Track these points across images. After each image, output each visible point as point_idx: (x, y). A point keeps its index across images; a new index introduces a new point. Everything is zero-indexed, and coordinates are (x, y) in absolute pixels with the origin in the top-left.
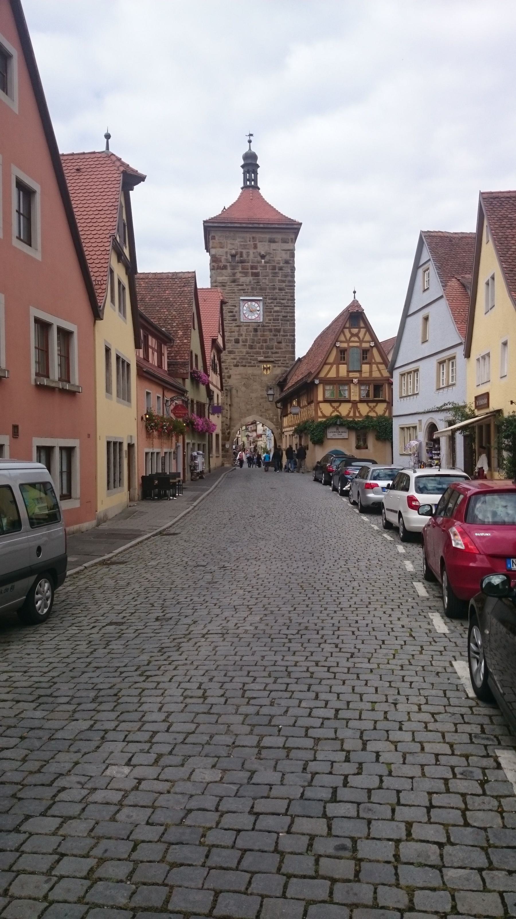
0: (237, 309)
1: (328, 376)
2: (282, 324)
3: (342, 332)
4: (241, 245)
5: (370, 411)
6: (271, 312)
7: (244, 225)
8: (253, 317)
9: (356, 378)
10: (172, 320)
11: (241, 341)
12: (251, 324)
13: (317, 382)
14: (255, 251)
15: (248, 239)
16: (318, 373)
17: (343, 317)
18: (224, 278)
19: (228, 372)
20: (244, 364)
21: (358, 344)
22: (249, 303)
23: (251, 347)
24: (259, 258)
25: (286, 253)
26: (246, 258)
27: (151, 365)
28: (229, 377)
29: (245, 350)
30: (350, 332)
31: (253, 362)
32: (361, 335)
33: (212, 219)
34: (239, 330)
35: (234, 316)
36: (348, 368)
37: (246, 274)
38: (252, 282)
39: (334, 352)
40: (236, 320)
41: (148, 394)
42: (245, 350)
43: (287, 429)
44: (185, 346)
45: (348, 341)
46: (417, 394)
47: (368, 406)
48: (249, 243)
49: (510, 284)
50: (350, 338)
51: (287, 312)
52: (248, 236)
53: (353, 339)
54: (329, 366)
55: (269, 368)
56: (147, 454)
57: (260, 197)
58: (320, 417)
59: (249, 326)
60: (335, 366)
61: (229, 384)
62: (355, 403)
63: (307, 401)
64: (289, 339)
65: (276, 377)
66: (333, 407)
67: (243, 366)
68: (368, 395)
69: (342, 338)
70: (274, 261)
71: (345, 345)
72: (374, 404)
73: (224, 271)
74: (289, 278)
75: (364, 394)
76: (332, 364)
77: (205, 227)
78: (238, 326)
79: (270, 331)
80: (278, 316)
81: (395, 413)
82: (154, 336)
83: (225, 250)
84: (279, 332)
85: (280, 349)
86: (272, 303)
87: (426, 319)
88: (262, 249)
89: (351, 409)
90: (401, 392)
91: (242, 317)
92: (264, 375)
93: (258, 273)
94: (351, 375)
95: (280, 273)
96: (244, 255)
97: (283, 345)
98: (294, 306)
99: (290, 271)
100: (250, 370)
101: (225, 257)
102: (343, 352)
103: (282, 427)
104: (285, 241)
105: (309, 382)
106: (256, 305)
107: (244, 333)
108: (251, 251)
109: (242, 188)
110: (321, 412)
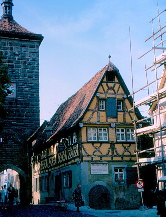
6: (22, 92)
13: (81, 125)
15: (6, 44)
17: (96, 79)
30: (107, 85)
32: (116, 89)
36: (106, 114)
39: (95, 100)
45: (105, 92)
47: (123, 146)
48: (7, 46)
50: (108, 90)
53: (109, 91)
54: (92, 112)
64: (35, 110)
69: (101, 90)
70: (25, 58)
72: (128, 145)
79: (22, 104)
86: (23, 85)
93: (13, 65)
96: (3, 54)
98: (39, 89)
104: (33, 47)
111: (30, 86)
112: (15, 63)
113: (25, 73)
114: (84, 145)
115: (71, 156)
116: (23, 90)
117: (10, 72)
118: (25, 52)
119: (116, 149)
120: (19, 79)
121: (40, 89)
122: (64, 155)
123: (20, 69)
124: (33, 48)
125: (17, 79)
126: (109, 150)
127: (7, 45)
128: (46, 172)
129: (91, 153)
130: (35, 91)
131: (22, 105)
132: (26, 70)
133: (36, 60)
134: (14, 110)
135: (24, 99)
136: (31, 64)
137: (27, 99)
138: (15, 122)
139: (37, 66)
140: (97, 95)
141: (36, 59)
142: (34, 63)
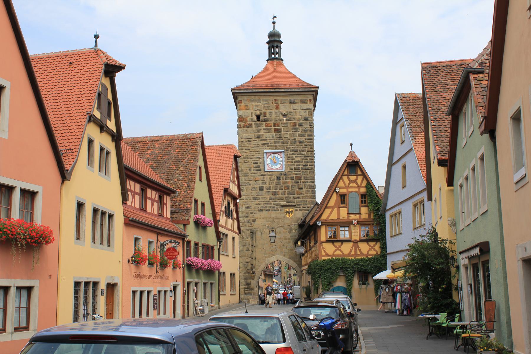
0: (261, 161)
1: (329, 219)
2: (302, 172)
4: (265, 107)
5: (370, 250)
6: (292, 163)
8: (277, 167)
9: (355, 220)
11: (264, 189)
13: (319, 224)
14: (277, 111)
18: (250, 134)
20: (268, 208)
21: (356, 189)
22: (273, 155)
23: (274, 194)
24: (281, 117)
27: (150, 214)
28: (254, 221)
29: (269, 196)
30: (349, 179)
31: (276, 206)
32: (359, 181)
33: (239, 86)
34: (264, 178)
35: (259, 167)
36: (348, 210)
37: (269, 131)
39: (335, 196)
40: (260, 170)
41: (136, 240)
42: (269, 196)
44: (188, 196)
46: (402, 233)
49: (435, 139)
50: (349, 184)
51: (307, 162)
52: (271, 98)
53: (351, 185)
55: (292, 212)
56: (134, 292)
58: (323, 256)
59: (272, 175)
60: (335, 209)
61: (254, 227)
62: (356, 242)
64: (309, 185)
65: (298, 220)
66: (336, 247)
67: (267, 210)
69: (341, 184)
72: (374, 243)
73: (249, 129)
74: (309, 133)
75: (363, 234)
76: (333, 208)
78: (262, 175)
80: (299, 165)
81: (388, 252)
82: (153, 188)
84: (300, 179)
85: (301, 194)
86: (293, 154)
87: (404, 167)
88: (284, 109)
89: (352, 247)
90: (391, 232)
93: (280, 129)
94: (352, 217)
95: (300, 129)
96: (268, 115)
97: (304, 190)
98: (313, 157)
99: (309, 127)
100: (273, 214)
102: (343, 196)
105: (311, 224)
106: (279, 157)
107: (268, 182)
108: (274, 111)
109: (267, 61)
110: (325, 251)
111: (302, 155)
113: (296, 138)
114: (324, 244)
116: (294, 161)
119: (350, 249)
120: (288, 147)
123: (289, 133)
124: (305, 103)
125: (286, 147)
126: (352, 249)
127: (272, 103)
129: (330, 253)
130: (308, 160)
131: (293, 179)
134: (282, 186)
135: (294, 171)
136: (303, 125)
137: (300, 172)
138: (285, 201)
140: (336, 191)
141: (309, 117)
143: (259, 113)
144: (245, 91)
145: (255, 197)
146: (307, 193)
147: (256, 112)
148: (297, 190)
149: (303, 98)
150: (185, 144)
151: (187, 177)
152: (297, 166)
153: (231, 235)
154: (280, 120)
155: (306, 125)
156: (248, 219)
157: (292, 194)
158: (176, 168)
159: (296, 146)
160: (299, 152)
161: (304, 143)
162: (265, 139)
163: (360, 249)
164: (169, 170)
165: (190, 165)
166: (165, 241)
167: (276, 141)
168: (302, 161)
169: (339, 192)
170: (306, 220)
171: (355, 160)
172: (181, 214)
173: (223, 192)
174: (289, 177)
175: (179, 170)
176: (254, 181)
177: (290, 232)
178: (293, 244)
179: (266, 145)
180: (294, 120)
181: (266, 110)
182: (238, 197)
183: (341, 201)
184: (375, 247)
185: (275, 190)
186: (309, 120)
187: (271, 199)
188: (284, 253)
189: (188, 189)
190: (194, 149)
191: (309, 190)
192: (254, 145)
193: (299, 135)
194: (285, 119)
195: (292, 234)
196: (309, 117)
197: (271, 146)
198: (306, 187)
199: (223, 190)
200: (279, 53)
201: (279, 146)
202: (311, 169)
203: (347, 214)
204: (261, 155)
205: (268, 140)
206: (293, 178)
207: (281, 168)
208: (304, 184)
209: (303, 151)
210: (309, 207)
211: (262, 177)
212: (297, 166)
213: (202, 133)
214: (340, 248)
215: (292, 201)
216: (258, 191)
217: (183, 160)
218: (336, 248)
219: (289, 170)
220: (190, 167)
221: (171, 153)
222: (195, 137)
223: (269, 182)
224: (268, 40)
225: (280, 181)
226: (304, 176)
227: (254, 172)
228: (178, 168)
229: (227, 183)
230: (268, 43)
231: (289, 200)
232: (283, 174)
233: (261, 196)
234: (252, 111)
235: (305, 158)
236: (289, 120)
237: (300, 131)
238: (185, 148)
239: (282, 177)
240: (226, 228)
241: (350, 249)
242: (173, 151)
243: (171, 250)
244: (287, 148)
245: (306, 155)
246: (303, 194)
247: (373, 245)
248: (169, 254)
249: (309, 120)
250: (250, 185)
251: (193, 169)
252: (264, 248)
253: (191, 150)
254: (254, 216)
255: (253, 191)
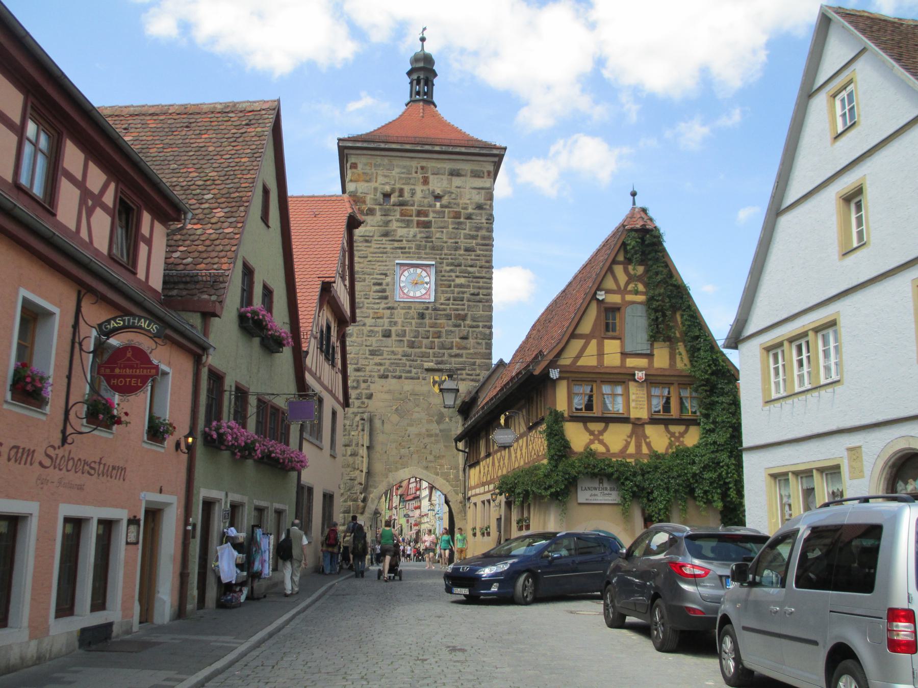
0: (388, 279)
1: (580, 363)
2: (469, 306)
3: (610, 270)
4: (400, 178)
6: (450, 286)
7: (408, 147)
8: (418, 294)
9: (640, 370)
10: (204, 187)
12: (413, 306)
13: (554, 374)
14: (425, 188)
15: (414, 170)
16: (559, 355)
19: (368, 388)
20: (398, 374)
22: (412, 270)
23: (412, 345)
24: (431, 199)
25: (479, 193)
26: (408, 199)
28: (370, 397)
29: (400, 350)
30: (626, 271)
31: (414, 371)
33: (353, 137)
34: (392, 314)
35: (384, 291)
36: (622, 346)
37: (408, 224)
38: (419, 236)
39: (593, 311)
40: (386, 298)
42: (400, 350)
43: (477, 491)
51: (479, 288)
52: (414, 164)
57: (436, 116)
59: (410, 308)
61: (368, 409)
62: (638, 425)
63: (527, 423)
64: (481, 332)
66: (591, 433)
67: (395, 377)
68: (667, 407)
69: (610, 283)
70: (458, 205)
71: (615, 299)
72: (681, 428)
74: (483, 233)
75: (658, 404)
76: (587, 338)
77: (339, 147)
78: (389, 308)
80: (463, 293)
83: (373, 185)
85: (465, 348)
86: (451, 271)
88: (437, 184)
89: (630, 436)
91: (397, 292)
92: (434, 394)
93: (430, 222)
94: (631, 362)
96: (407, 195)
97: (471, 341)
99: (484, 221)
100: (408, 386)
101: (372, 196)
102: (610, 312)
103: (465, 489)
104: (476, 175)
105: (537, 373)
106: (424, 274)
107: (400, 321)
108: (419, 189)
111: (470, 273)
112: (435, 215)
113: (459, 240)
115: (535, 454)
116: (453, 283)
117: (421, 240)
118: (457, 187)
120: (443, 256)
121: (494, 281)
122: (521, 450)
123: (445, 230)
124: (479, 177)
125: (438, 257)
127: (416, 172)
128: (489, 491)
130: (481, 284)
131: (450, 319)
132: (460, 233)
133: (485, 207)
135: (453, 304)
136: (474, 217)
138: (432, 361)
139: (487, 223)
140: (598, 297)
141: (485, 204)
142: (481, 214)
143: (389, 190)
144: (365, 145)
145: (373, 350)
146: (476, 346)
147: (382, 186)
148: (458, 340)
149: (476, 167)
150: (229, 123)
151: (227, 195)
152: (459, 293)
153: (329, 403)
154: (430, 206)
155: (478, 218)
156: (358, 391)
157: (447, 347)
158: (196, 174)
159: (457, 256)
160: (463, 267)
161: (474, 251)
162: (398, 239)
163: (648, 440)
164: (175, 179)
165: (237, 168)
166: (108, 321)
167: (420, 245)
168: (470, 286)
169: (603, 300)
170: (479, 394)
171: (647, 227)
172: (198, 286)
173: (319, 290)
174: (440, 315)
175: (205, 179)
176: (373, 318)
177: (439, 422)
178: (445, 446)
179: (400, 251)
180: (455, 206)
181: (403, 184)
182: (348, 320)
183: (607, 325)
184: (683, 437)
185: (414, 337)
186: (485, 209)
187: (405, 355)
188: (424, 463)
189: (226, 224)
190: (253, 134)
191: (480, 341)
192: (377, 248)
193: (465, 235)
194: (438, 204)
195: (442, 426)
196: (485, 204)
197: (409, 253)
198: (475, 336)
199: (320, 286)
200: (429, 93)
201: (426, 254)
202: (486, 302)
203: (622, 353)
204: (388, 270)
205: (404, 242)
206: (451, 316)
207: (426, 296)
208: (471, 329)
209: (471, 266)
210: (479, 375)
211: (389, 311)
212: (459, 293)
213: (279, 101)
214: (601, 437)
215: (447, 360)
216: (381, 338)
217: (218, 157)
218: (592, 437)
219: (442, 301)
220: (236, 173)
221: (187, 141)
222: (259, 109)
223: (403, 322)
224: (409, 67)
225: (425, 320)
226: (471, 315)
227: (374, 301)
228: (202, 175)
229: (331, 272)
230: (409, 73)
231: (440, 359)
232: (430, 308)
233: (385, 349)
234: (377, 185)
235: (474, 280)
236: (446, 207)
237: (467, 229)
238: (226, 131)
239: (429, 314)
240: (319, 380)
241: (626, 441)
242: (193, 136)
243: (129, 355)
244: (440, 259)
245: (477, 275)
246: (469, 349)
247: (679, 433)
248: (117, 371)
249: (485, 209)
250: (364, 325)
251: (245, 177)
252: (386, 452)
253: (244, 135)
254: (369, 386)
255: (370, 339)
